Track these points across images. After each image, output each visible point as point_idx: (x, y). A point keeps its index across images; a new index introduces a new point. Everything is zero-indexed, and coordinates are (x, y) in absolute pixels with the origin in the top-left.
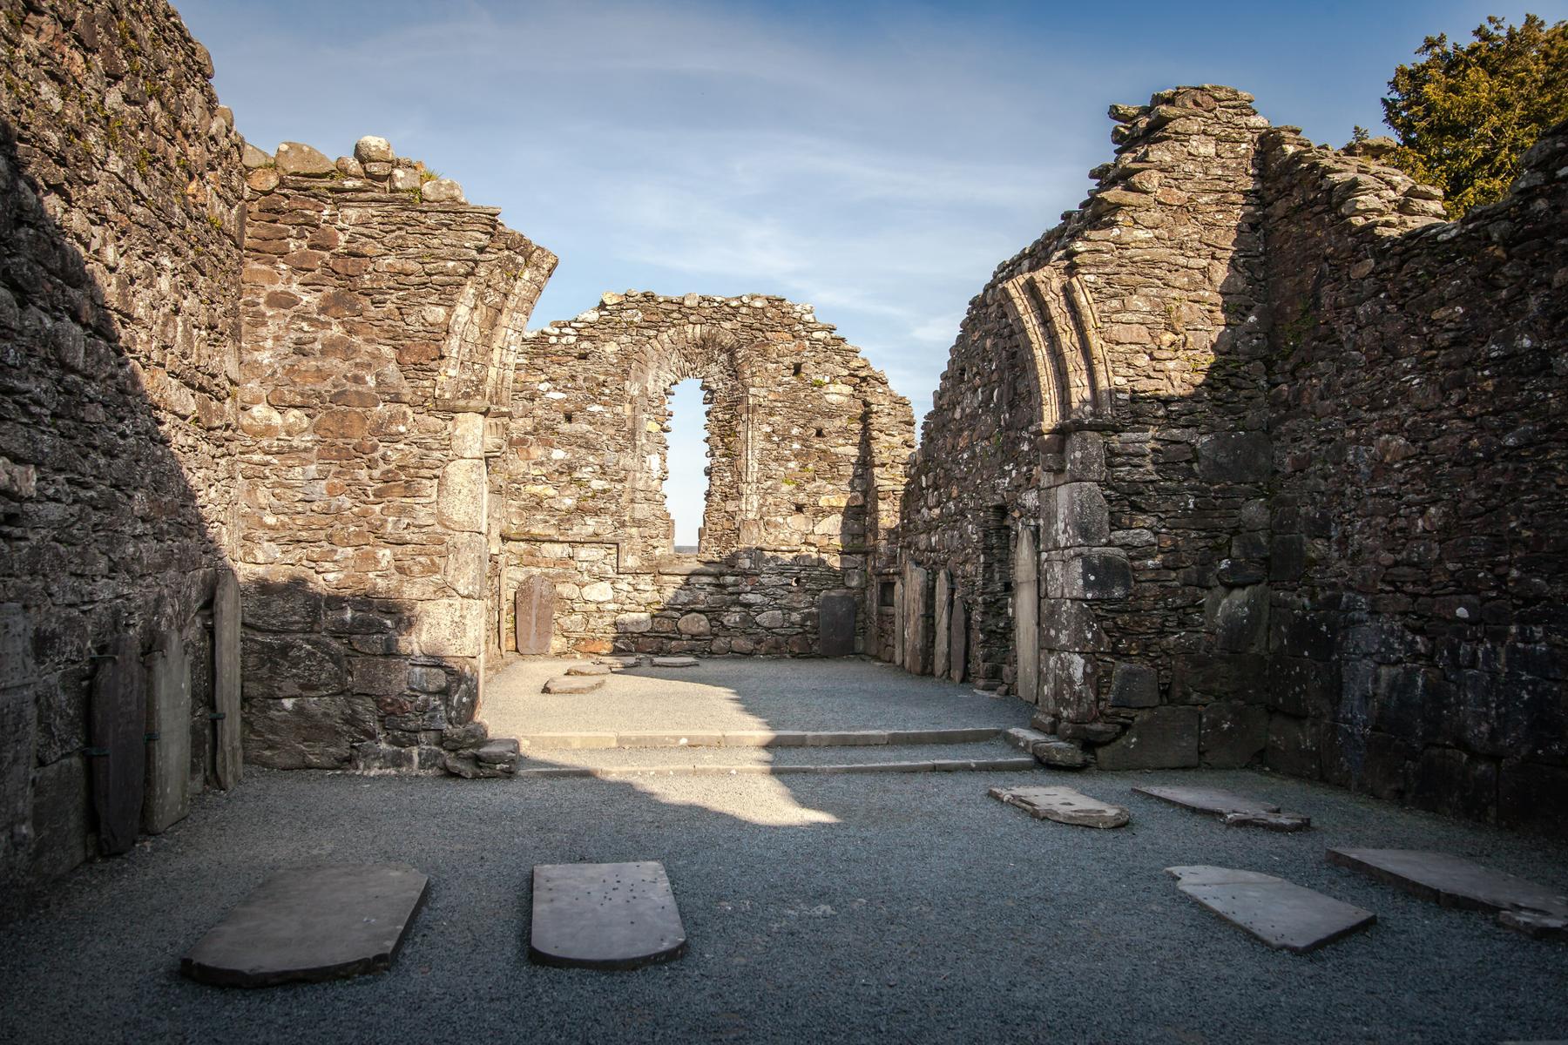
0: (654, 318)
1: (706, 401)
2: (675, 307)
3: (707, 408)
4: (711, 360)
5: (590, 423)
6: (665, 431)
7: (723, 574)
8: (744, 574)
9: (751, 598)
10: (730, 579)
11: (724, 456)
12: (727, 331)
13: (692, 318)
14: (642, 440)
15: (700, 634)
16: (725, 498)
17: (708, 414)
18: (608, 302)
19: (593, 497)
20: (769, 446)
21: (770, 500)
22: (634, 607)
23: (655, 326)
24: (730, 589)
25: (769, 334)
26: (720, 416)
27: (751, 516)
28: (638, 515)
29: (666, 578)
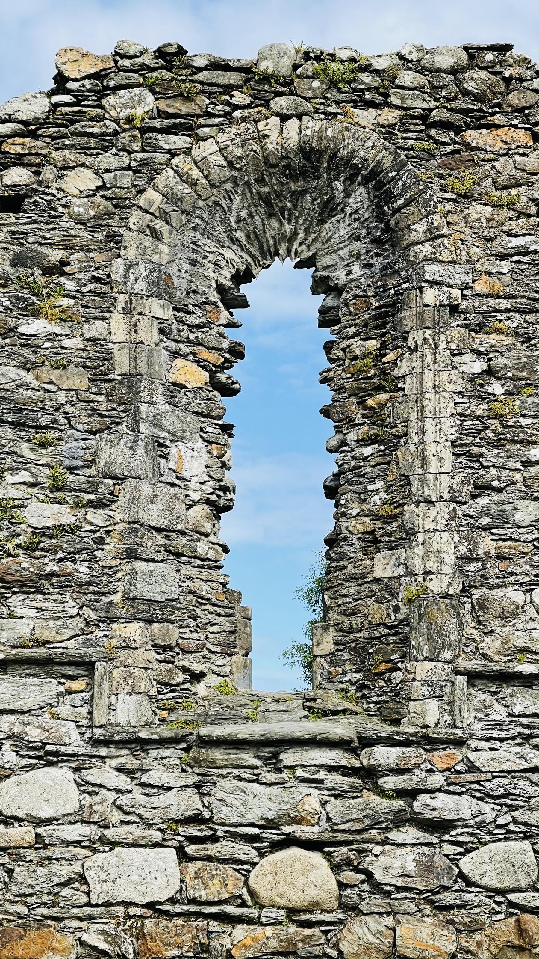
0: (184, 108)
1: (327, 318)
2: (234, 78)
3: (327, 334)
4: (329, 209)
5: (28, 366)
6: (229, 390)
7: (367, 742)
8: (427, 741)
9: (445, 805)
10: (385, 756)
11: (363, 442)
12: (362, 133)
13: (281, 104)
14: (154, 403)
15: (314, 906)
16: (372, 542)
17: (328, 347)
18: (71, 71)
19: (30, 548)
20: (481, 409)
21: (487, 544)
22: (135, 831)
23: (186, 126)
24: (389, 782)
25: (471, 136)
26: (357, 346)
27: (436, 585)
28: (143, 589)
29: (217, 754)
